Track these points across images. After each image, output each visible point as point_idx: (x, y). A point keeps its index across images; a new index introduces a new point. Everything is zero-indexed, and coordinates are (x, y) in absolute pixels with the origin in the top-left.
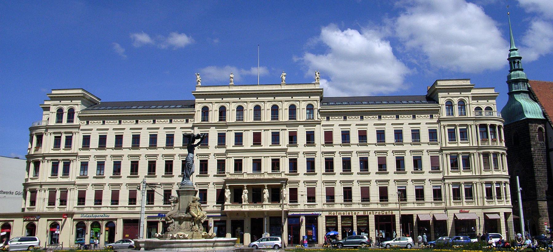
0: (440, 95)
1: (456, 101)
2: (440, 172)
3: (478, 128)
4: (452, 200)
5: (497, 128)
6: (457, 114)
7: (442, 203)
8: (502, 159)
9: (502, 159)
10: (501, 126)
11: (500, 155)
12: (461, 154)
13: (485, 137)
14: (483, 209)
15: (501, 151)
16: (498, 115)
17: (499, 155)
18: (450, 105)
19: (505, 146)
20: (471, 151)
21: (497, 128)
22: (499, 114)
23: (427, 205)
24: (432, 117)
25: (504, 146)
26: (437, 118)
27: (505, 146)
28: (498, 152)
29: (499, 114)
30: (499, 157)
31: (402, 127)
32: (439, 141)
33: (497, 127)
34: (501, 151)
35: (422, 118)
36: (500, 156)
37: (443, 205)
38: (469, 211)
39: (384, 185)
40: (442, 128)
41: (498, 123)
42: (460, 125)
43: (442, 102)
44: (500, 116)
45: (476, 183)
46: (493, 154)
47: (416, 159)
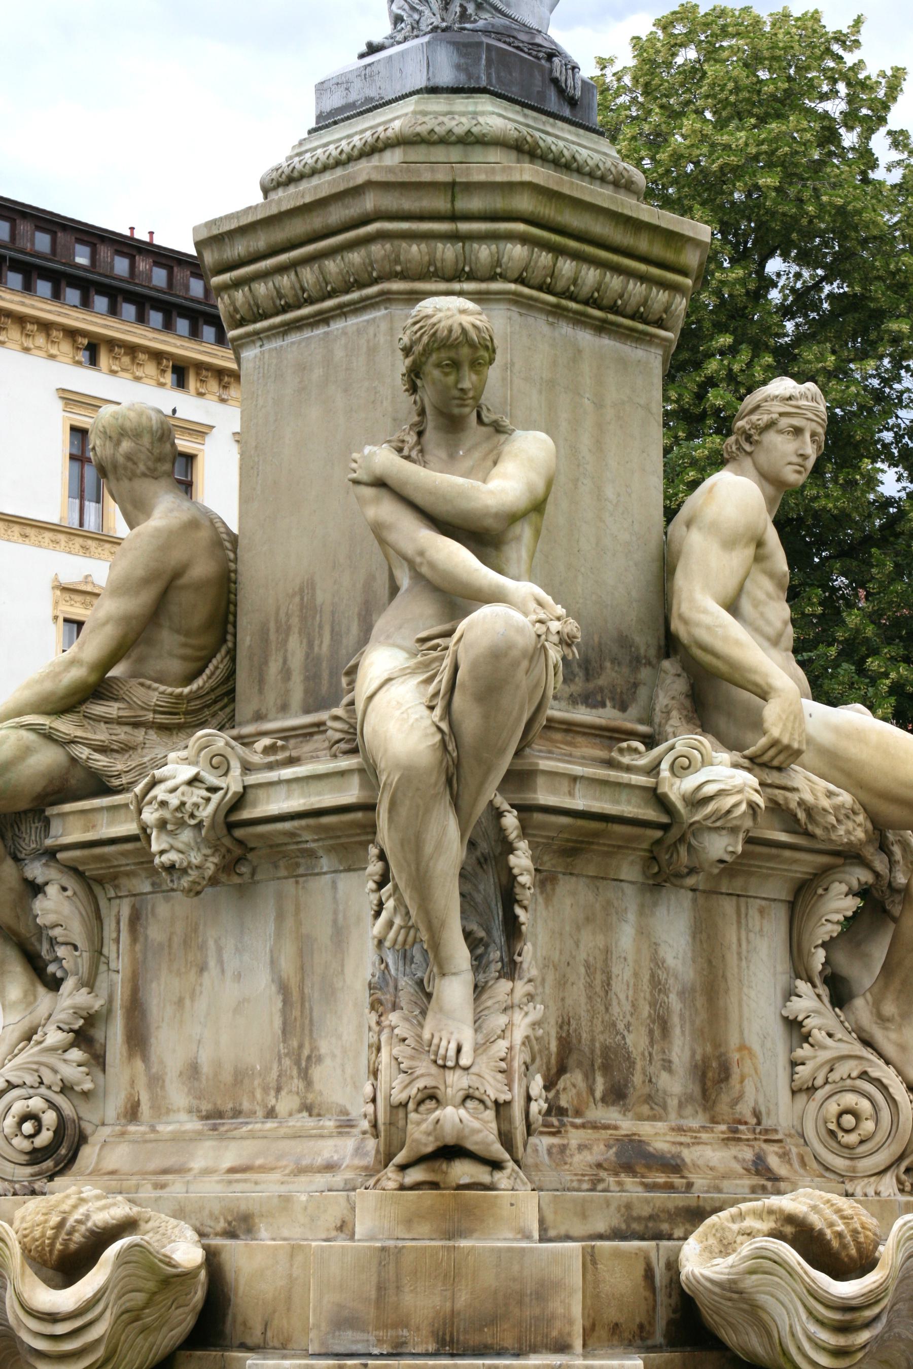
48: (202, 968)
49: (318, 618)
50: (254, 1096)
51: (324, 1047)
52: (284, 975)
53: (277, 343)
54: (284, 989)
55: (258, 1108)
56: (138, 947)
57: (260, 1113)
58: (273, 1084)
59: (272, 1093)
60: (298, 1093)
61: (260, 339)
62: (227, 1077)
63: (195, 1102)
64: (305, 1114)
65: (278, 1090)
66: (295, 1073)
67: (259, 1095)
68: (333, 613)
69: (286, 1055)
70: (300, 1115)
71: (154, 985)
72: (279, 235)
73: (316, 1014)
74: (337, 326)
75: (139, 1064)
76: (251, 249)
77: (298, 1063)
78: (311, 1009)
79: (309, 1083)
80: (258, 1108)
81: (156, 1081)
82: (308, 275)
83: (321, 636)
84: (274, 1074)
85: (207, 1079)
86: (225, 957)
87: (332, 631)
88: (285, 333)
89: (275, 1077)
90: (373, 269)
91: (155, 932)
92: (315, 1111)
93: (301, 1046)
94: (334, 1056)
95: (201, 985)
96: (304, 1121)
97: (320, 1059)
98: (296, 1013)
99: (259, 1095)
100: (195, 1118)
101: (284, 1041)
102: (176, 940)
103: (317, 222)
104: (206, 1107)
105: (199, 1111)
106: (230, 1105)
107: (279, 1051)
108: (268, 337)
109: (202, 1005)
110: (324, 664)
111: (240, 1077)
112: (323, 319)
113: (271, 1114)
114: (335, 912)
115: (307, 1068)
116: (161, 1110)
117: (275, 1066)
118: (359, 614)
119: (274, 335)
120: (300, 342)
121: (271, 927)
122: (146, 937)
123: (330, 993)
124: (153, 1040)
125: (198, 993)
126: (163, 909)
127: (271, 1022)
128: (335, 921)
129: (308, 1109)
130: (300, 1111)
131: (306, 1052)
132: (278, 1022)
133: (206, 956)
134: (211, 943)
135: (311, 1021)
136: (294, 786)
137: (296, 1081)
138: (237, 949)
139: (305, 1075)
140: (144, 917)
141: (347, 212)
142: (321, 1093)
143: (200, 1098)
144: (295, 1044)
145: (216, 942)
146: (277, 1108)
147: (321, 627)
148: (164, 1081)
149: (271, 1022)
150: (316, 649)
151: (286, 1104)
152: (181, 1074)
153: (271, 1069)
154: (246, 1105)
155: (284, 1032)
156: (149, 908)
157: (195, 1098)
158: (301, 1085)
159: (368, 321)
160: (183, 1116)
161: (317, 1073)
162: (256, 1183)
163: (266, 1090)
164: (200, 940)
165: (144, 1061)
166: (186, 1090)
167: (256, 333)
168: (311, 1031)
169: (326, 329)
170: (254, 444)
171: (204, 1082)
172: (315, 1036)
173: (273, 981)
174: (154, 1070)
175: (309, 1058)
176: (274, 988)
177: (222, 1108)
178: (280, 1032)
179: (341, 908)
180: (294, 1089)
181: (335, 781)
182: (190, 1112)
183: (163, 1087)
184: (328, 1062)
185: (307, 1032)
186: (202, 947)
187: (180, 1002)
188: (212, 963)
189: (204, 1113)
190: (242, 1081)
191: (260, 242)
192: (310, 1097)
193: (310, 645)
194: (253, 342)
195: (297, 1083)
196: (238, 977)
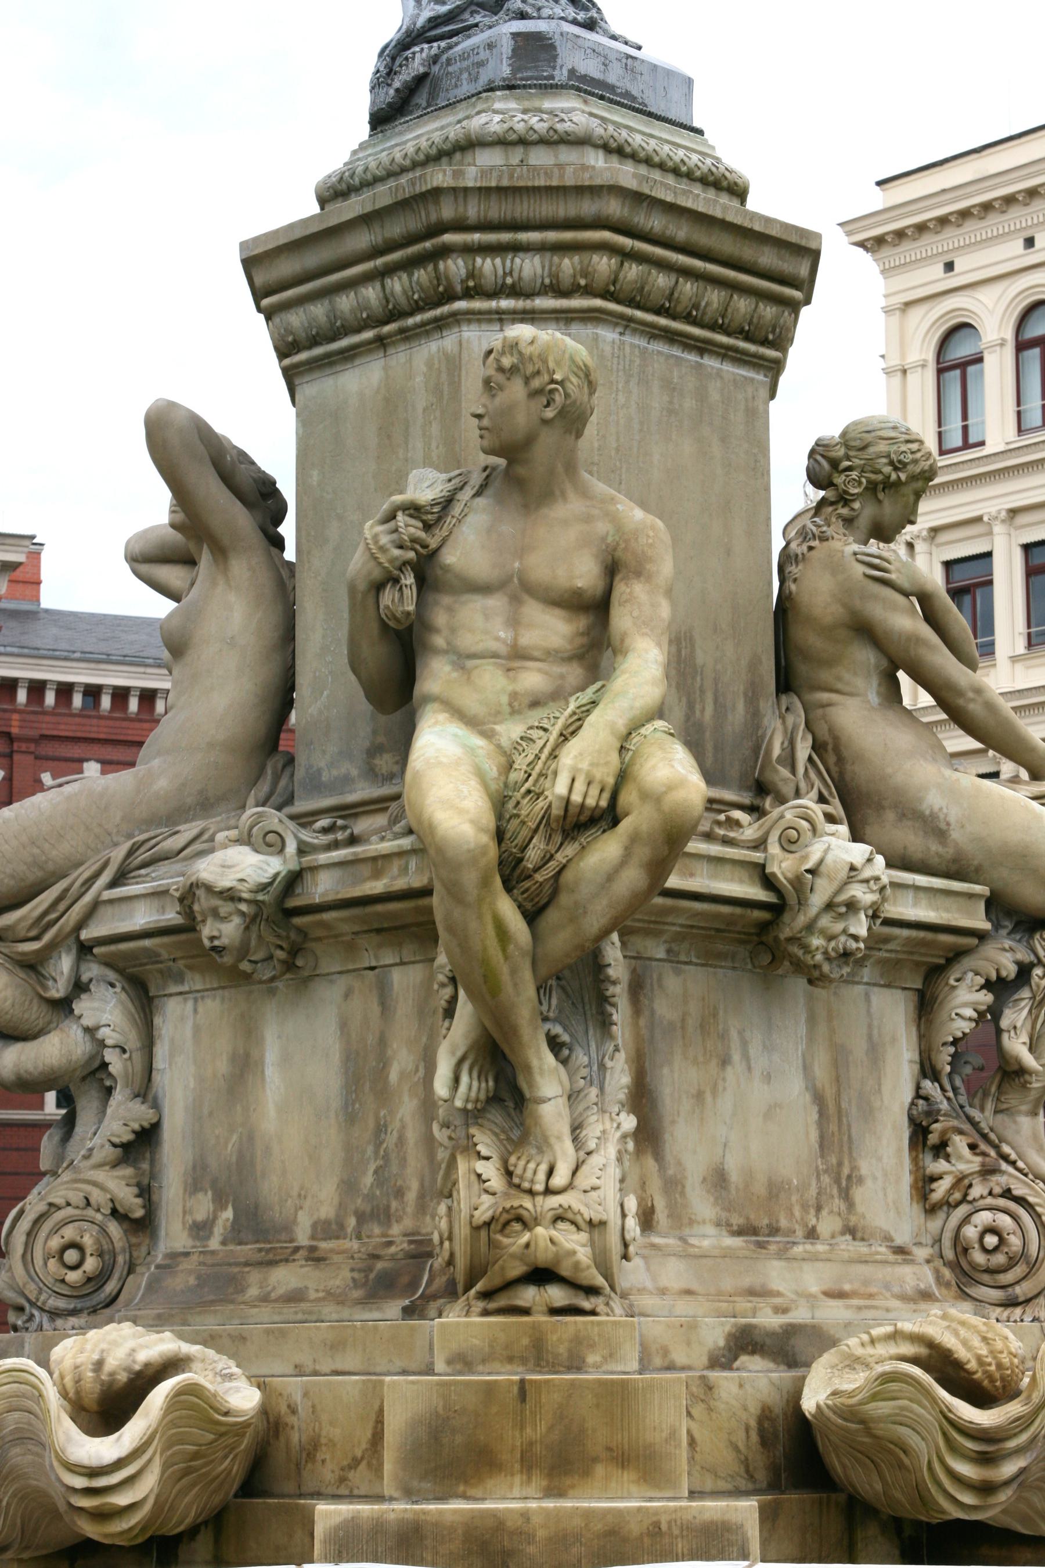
48: (725, 1062)
49: (698, 679)
50: (792, 1214)
51: (865, 1167)
52: (819, 1085)
53: (641, 342)
54: (819, 1099)
55: (797, 1227)
56: (642, 1022)
57: (800, 1233)
58: (812, 1202)
59: (812, 1211)
60: (839, 1214)
61: (626, 327)
62: (760, 1188)
63: (724, 1215)
64: (848, 1237)
65: (819, 1209)
66: (835, 1191)
67: (797, 1212)
68: (716, 681)
69: (826, 1171)
70: (843, 1238)
71: (666, 1071)
72: (705, 239)
73: (854, 1131)
74: (711, 363)
75: (650, 1163)
76: (668, 233)
77: (837, 1181)
78: (849, 1126)
79: (851, 1205)
80: (797, 1227)
81: (673, 1186)
82: (714, 297)
83: (702, 701)
84: (813, 1191)
85: (737, 1189)
86: (752, 1052)
87: (716, 701)
88: (653, 337)
89: (815, 1195)
90: (773, 332)
91: (664, 1008)
92: (859, 1235)
93: (840, 1164)
94: (875, 1178)
95: (724, 1079)
96: (846, 1245)
97: (860, 1180)
98: (833, 1127)
99: (797, 1212)
100: (725, 1233)
101: (822, 1157)
102: (690, 1022)
103: (747, 252)
104: (737, 1221)
105: (729, 1225)
106: (766, 1221)
107: (817, 1167)
108: (635, 330)
109: (726, 1103)
110: (708, 734)
111: (775, 1190)
112: (702, 348)
113: (812, 1234)
114: (870, 1026)
115: (848, 1189)
116: (681, 1219)
117: (814, 1182)
118: (745, 695)
119: (643, 332)
120: (669, 357)
121: (802, 1030)
122: (653, 1012)
123: (868, 1112)
124: (667, 1136)
125: (721, 1089)
126: (672, 983)
127: (807, 1133)
128: (870, 1037)
129: (852, 1231)
130: (843, 1234)
131: (846, 1171)
132: (814, 1135)
133: (729, 1047)
134: (734, 1034)
135: (850, 1137)
136: (922, 895)
137: (837, 1201)
138: (764, 1046)
139: (846, 1195)
140: (648, 986)
141: (780, 263)
142: (864, 1217)
143: (729, 1211)
144: (834, 1160)
145: (740, 1033)
146: (819, 1229)
147: (702, 691)
148: (684, 1187)
149: (807, 1133)
150: (698, 713)
151: (827, 1225)
152: (704, 1180)
153: (809, 1185)
154: (783, 1223)
155: (822, 1146)
156: (655, 977)
157: (723, 1209)
158: (843, 1207)
159: (745, 378)
160: (710, 1230)
161: (858, 1194)
162: (888, 1310)
163: (805, 1207)
164: (721, 1027)
165: (656, 1160)
166: (712, 1199)
167: (630, 319)
168: (850, 1149)
169: (698, 359)
170: (614, 445)
171: (734, 1192)
172: (854, 1155)
173: (807, 1088)
174: (670, 1172)
175: (849, 1177)
176: (808, 1097)
177: (756, 1223)
178: (817, 1146)
179: (875, 1023)
180: (836, 1210)
181: (962, 901)
182: (718, 1224)
183: (683, 1194)
184: (869, 1183)
185: (846, 1149)
186: (723, 1036)
187: (699, 1096)
188: (736, 1057)
189: (735, 1228)
190: (777, 1196)
191: (681, 232)
192: (853, 1220)
193: (691, 706)
194: (616, 324)
195: (838, 1204)
196: (768, 1078)
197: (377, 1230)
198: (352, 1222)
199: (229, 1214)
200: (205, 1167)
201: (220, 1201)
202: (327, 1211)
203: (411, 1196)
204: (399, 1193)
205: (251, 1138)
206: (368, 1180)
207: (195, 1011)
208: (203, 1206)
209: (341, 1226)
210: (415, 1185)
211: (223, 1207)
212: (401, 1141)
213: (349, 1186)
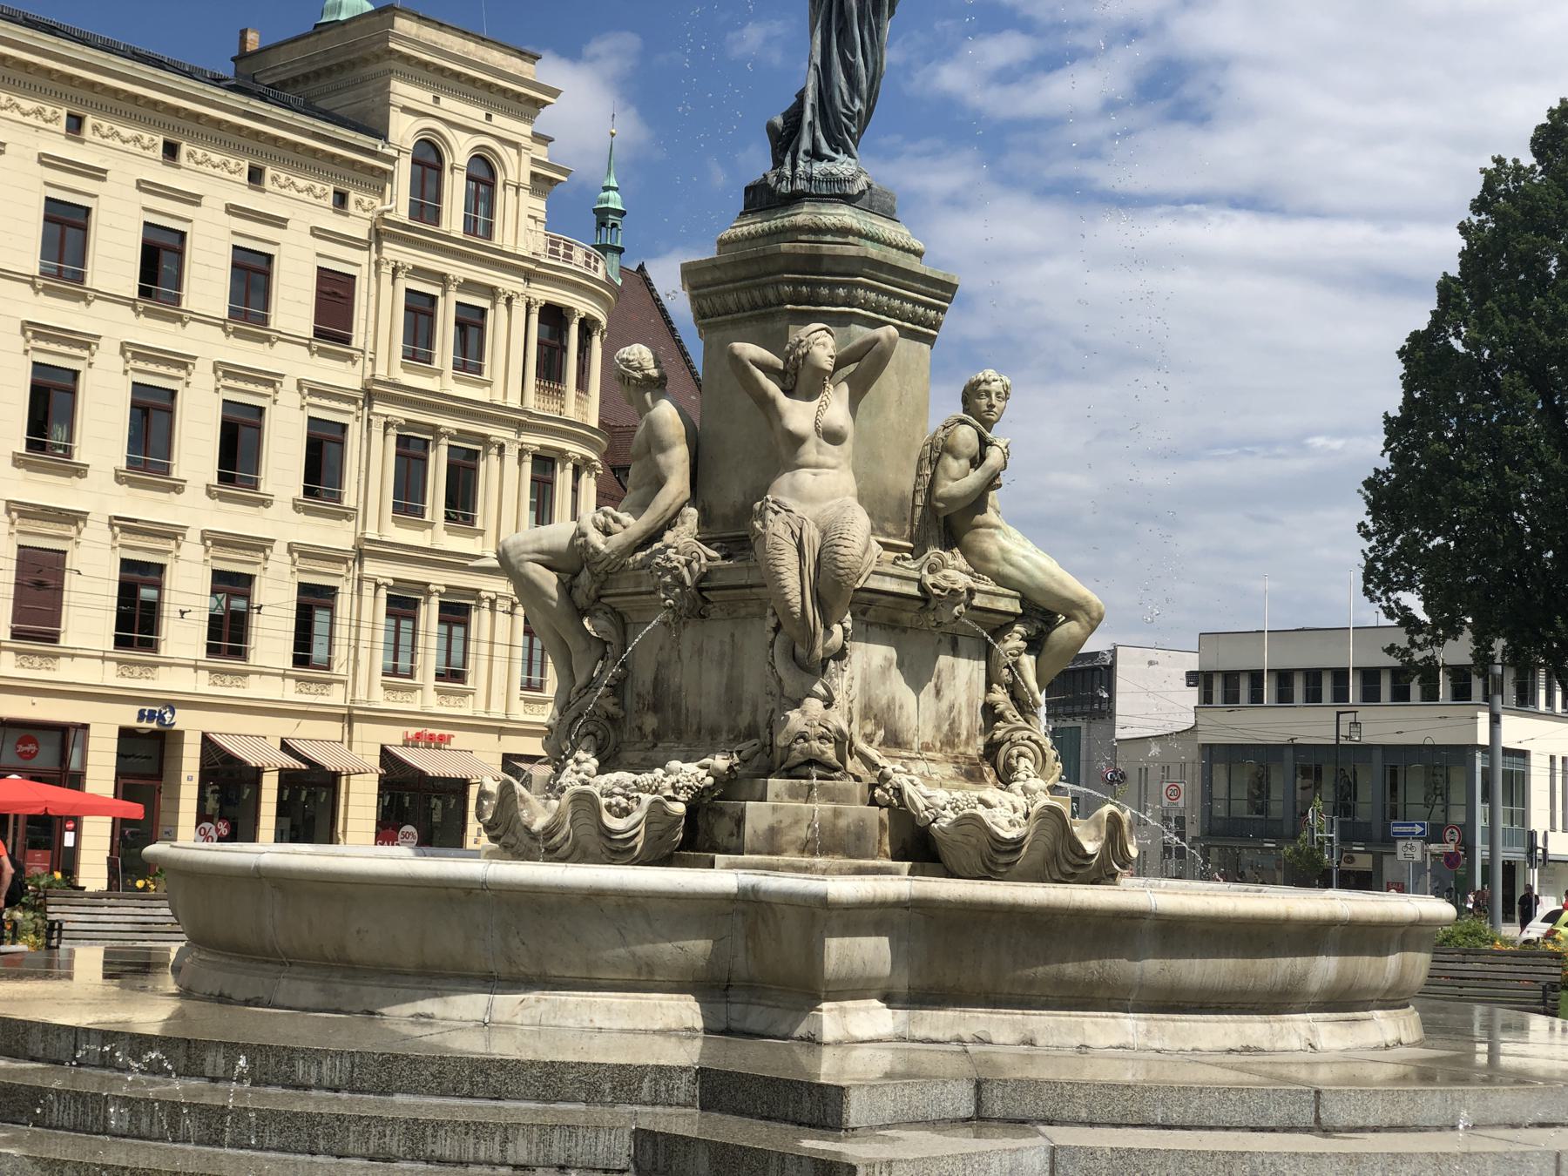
0: (403, 91)
1: (460, 149)
2: (346, 515)
3: (534, 319)
4: (378, 678)
5: (574, 330)
6: (453, 219)
7: (329, 682)
8: (575, 490)
9: (575, 490)
10: (596, 322)
11: (570, 465)
12: (451, 438)
13: (550, 369)
14: (501, 731)
15: (575, 449)
16: (588, 264)
17: (563, 469)
18: (429, 160)
19: (596, 427)
20: (496, 433)
21: (574, 330)
22: (596, 261)
23: (257, 689)
24: (341, 200)
25: (594, 423)
26: (368, 215)
27: (596, 427)
28: (562, 452)
29: (596, 261)
30: (563, 478)
31: (189, 216)
32: (361, 346)
33: (576, 321)
34: (575, 449)
35: (294, 193)
36: (569, 473)
37: (336, 697)
38: (450, 737)
39: (45, 537)
40: (386, 279)
41: (583, 306)
42: (468, 286)
43: (403, 131)
44: (596, 269)
45: (493, 596)
46: (536, 457)
47: (236, 416)
197: (949, 750)
198: (938, 745)
199: (881, 733)
200: (871, 708)
201: (878, 725)
202: (928, 739)
203: (963, 737)
204: (959, 735)
205: (894, 699)
206: (946, 727)
207: (867, 630)
208: (869, 728)
209: (934, 746)
210: (965, 733)
211: (880, 729)
212: (959, 712)
213: (938, 728)
